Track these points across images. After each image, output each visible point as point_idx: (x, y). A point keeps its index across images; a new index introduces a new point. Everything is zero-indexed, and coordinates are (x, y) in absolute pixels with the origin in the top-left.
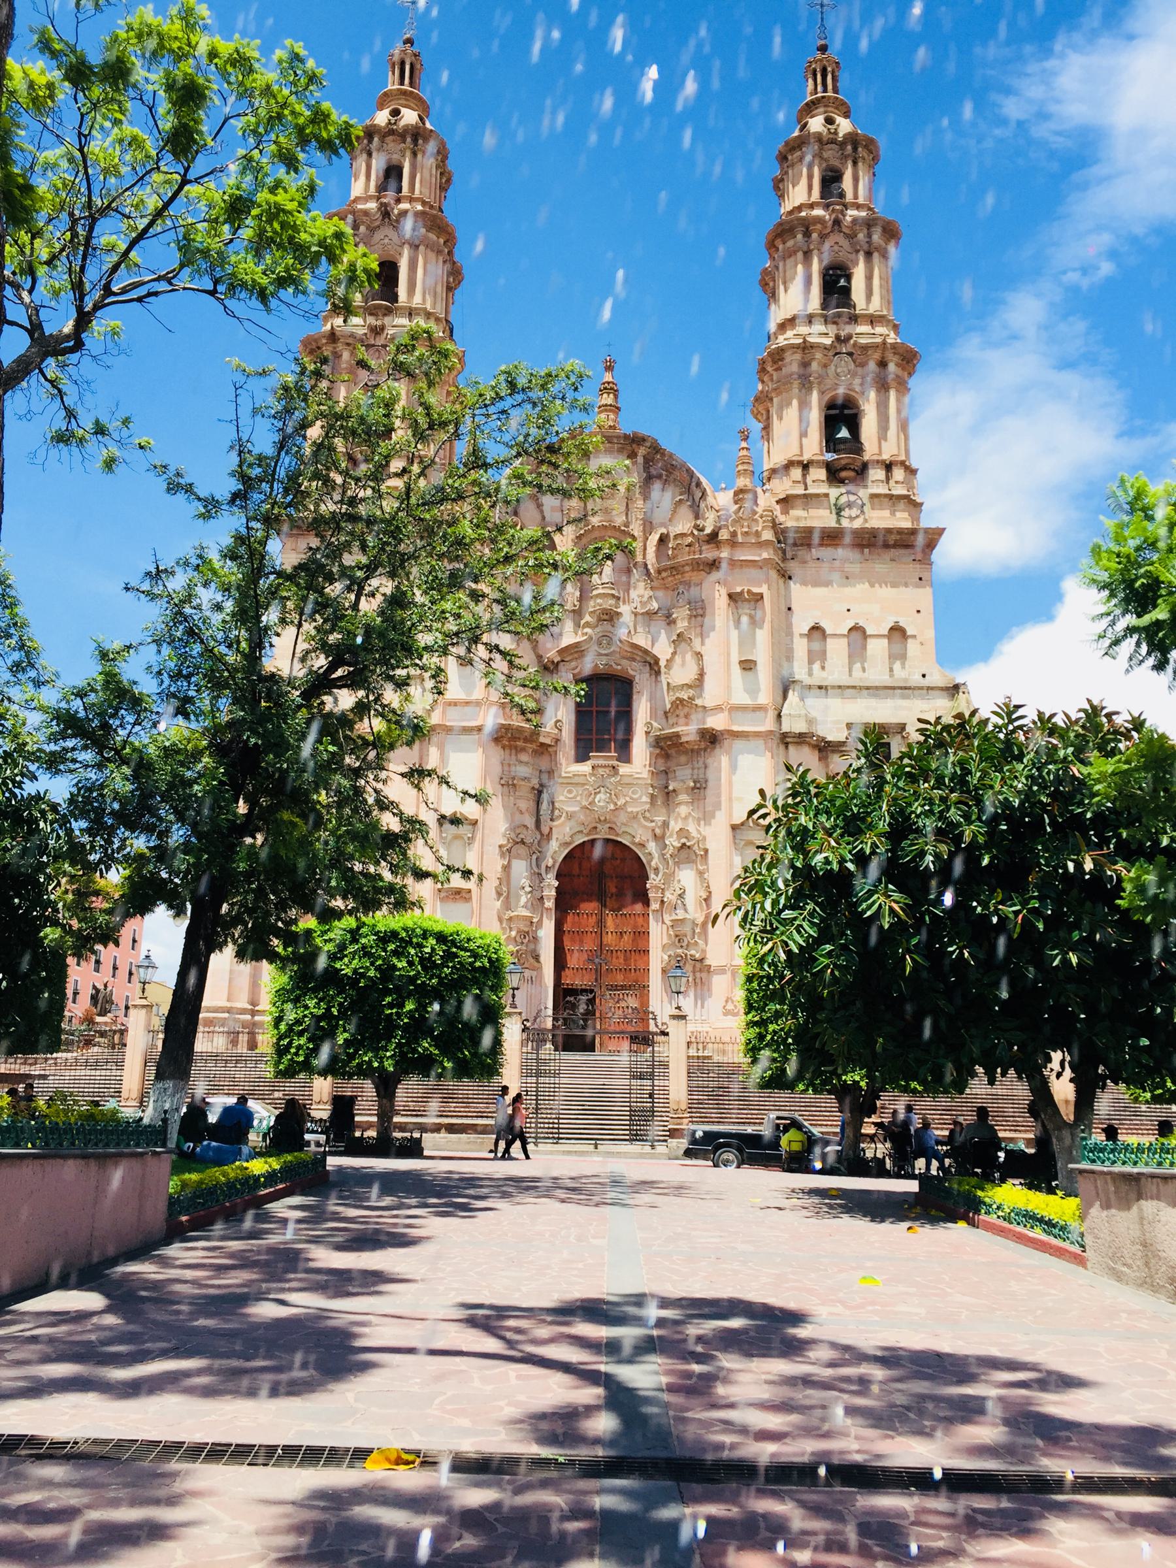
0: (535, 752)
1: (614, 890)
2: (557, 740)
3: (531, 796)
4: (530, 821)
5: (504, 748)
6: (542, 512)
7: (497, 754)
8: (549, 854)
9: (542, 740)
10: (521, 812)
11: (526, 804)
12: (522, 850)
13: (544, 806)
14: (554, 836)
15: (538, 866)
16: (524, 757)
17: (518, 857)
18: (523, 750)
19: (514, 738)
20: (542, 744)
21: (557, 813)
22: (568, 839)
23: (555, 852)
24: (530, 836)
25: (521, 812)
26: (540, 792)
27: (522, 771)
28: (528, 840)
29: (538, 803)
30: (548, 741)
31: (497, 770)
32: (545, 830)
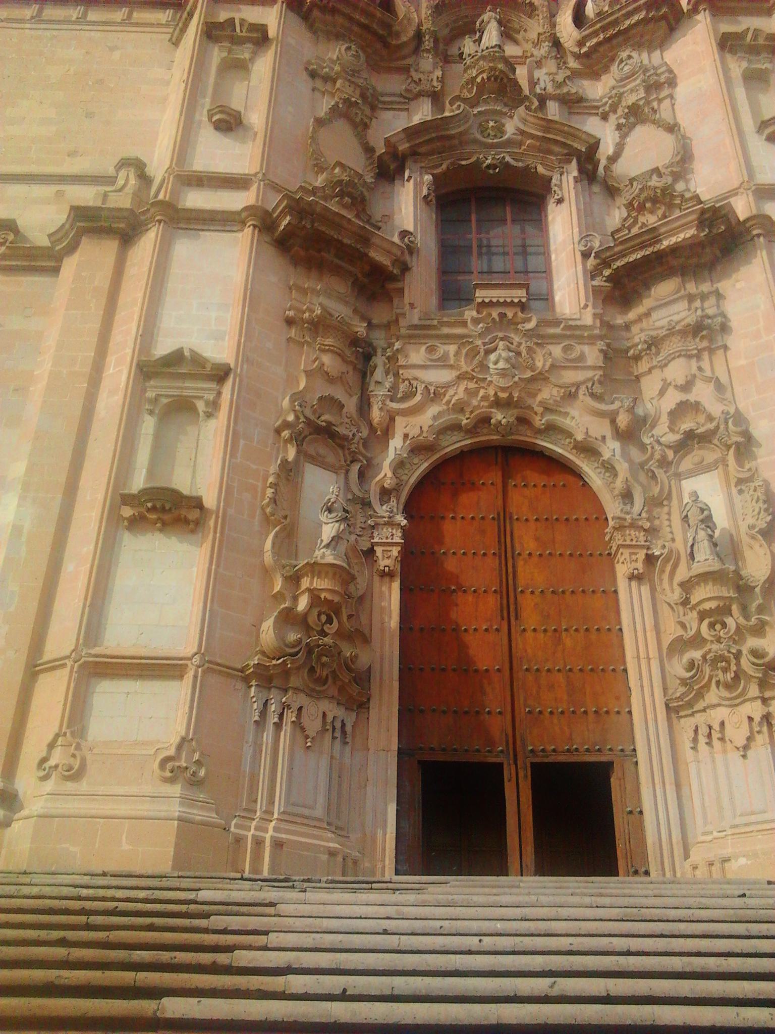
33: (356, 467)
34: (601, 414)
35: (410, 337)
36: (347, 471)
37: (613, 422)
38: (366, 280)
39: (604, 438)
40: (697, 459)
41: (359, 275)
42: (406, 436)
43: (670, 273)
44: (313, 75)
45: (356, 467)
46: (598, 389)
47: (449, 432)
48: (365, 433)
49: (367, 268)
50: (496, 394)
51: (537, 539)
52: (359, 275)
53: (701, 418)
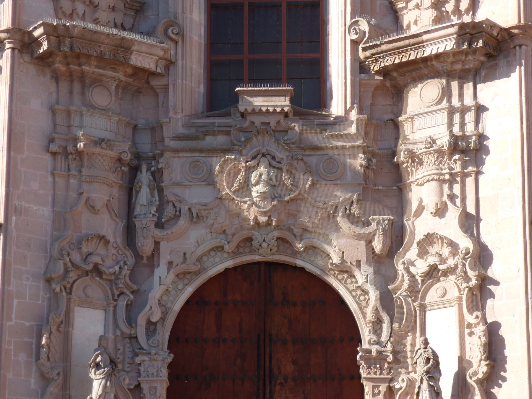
0: (123, 88)
1: (290, 368)
2: (170, 64)
3: (113, 178)
4: (110, 227)
5: (56, 78)
7: (41, 91)
8: (156, 293)
9: (137, 60)
10: (93, 209)
11: (104, 192)
12: (96, 289)
13: (144, 195)
14: (164, 258)
15: (131, 321)
16: (100, 97)
17: (88, 303)
18: (98, 82)
20: (138, 71)
21: (169, 211)
23: (167, 293)
24: (110, 258)
25: (93, 209)
26: (135, 170)
28: (110, 267)
29: (130, 191)
30: (149, 64)
31: (39, 122)
32: (146, 246)
34: (359, 237)
35: (175, 151)
36: (115, 307)
37: (369, 242)
38: (130, 80)
39: (358, 262)
40: (440, 292)
41: (123, 78)
42: (170, 263)
43: (436, 75)
45: (122, 303)
46: (355, 210)
47: (213, 253)
48: (131, 261)
49: (129, 71)
50: (256, 217)
51: (294, 363)
52: (123, 78)
53: (446, 251)
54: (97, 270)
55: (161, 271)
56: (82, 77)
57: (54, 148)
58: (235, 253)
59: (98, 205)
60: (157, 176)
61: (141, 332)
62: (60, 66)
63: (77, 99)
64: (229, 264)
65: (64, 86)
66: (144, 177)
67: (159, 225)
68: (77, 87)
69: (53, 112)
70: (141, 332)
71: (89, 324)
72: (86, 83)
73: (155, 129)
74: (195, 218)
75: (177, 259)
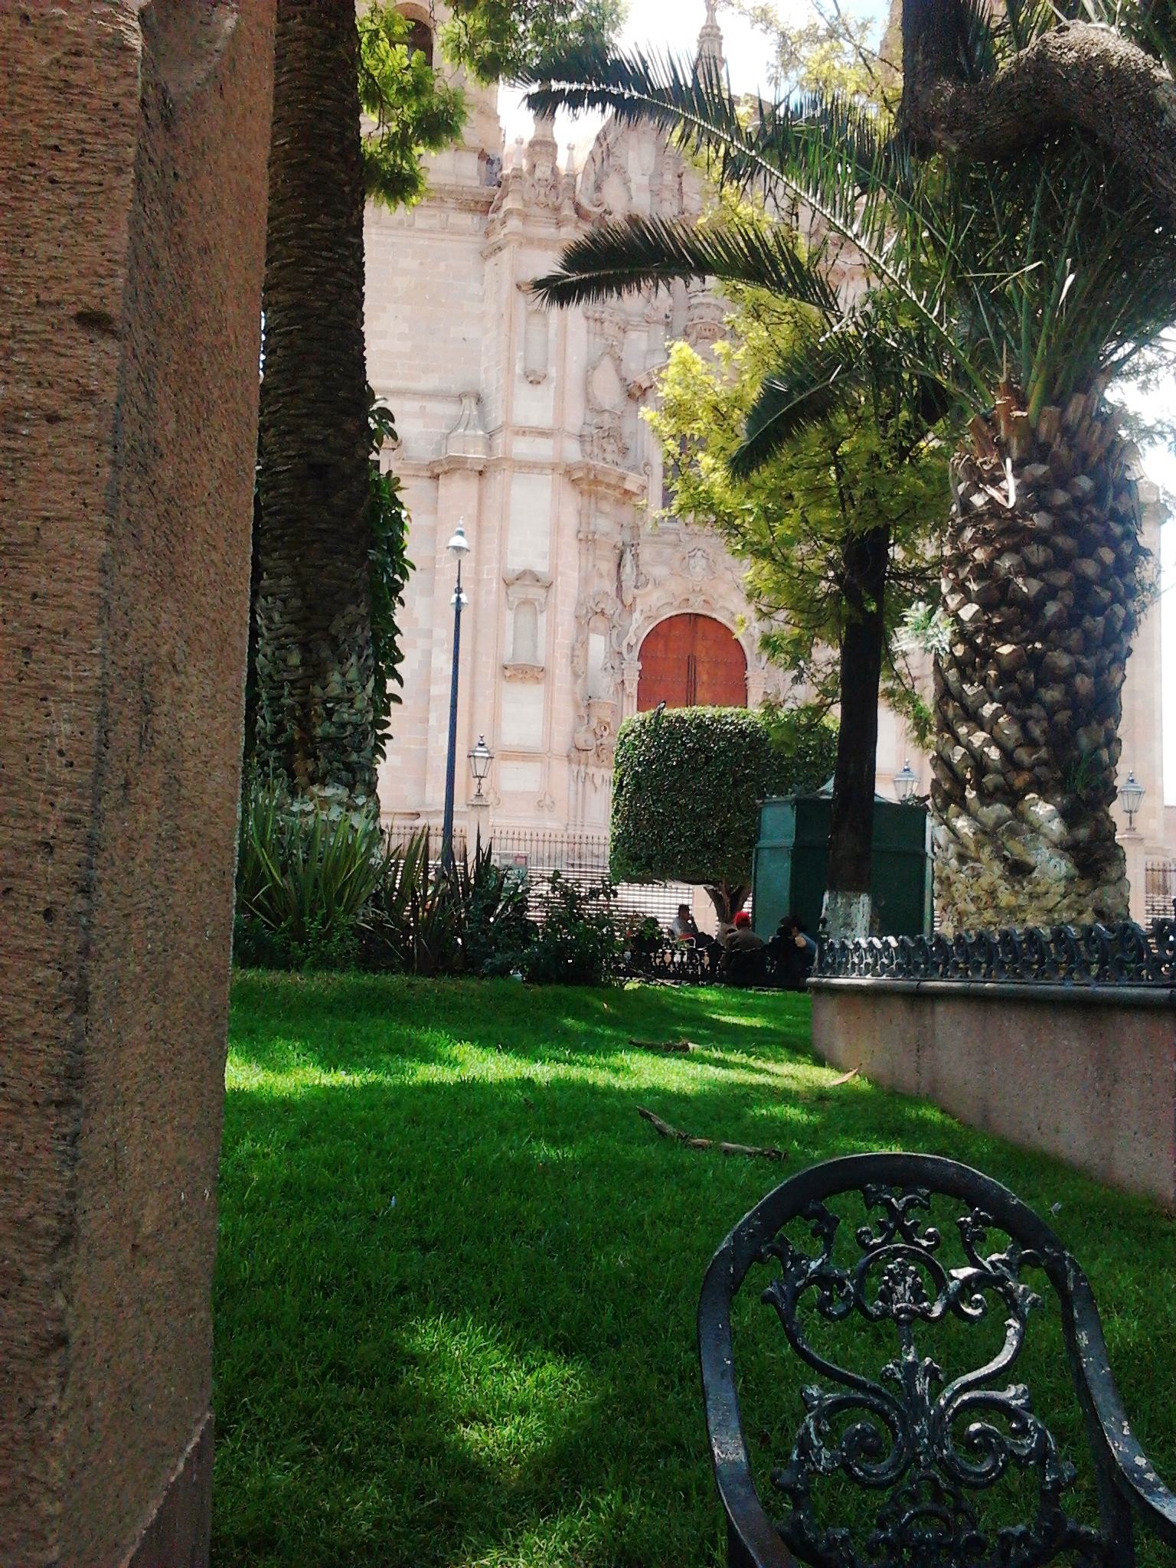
0: (617, 501)
1: (705, 677)
4: (610, 587)
6: (629, 190)
8: (632, 629)
10: (601, 576)
11: (607, 566)
12: (599, 623)
15: (620, 645)
16: (606, 507)
18: (605, 497)
19: (596, 481)
20: (626, 492)
21: (642, 579)
22: (654, 613)
23: (638, 628)
25: (601, 576)
27: (604, 525)
28: (609, 611)
31: (570, 521)
32: (628, 600)
33: (615, 632)
44: (587, 318)
54: (603, 613)
55: (636, 615)
56: (596, 494)
57: (581, 536)
58: (679, 607)
59: (605, 573)
60: (636, 556)
61: (624, 651)
62: (585, 487)
63: (593, 506)
64: (674, 613)
65: (586, 498)
66: (628, 557)
67: (636, 587)
68: (593, 499)
69: (580, 513)
70: (624, 651)
71: (598, 645)
72: (599, 498)
73: (635, 528)
74: (657, 584)
75: (646, 609)
